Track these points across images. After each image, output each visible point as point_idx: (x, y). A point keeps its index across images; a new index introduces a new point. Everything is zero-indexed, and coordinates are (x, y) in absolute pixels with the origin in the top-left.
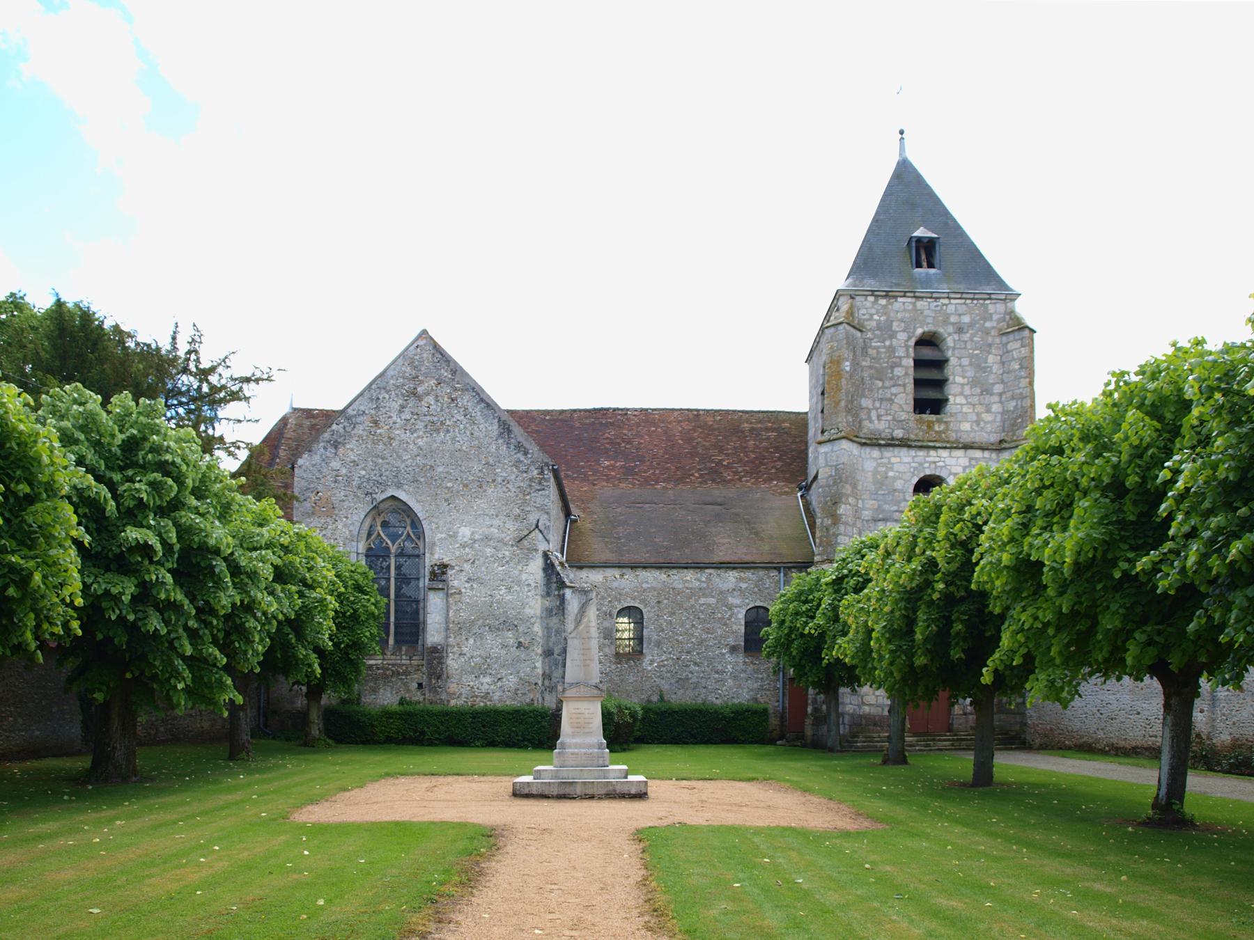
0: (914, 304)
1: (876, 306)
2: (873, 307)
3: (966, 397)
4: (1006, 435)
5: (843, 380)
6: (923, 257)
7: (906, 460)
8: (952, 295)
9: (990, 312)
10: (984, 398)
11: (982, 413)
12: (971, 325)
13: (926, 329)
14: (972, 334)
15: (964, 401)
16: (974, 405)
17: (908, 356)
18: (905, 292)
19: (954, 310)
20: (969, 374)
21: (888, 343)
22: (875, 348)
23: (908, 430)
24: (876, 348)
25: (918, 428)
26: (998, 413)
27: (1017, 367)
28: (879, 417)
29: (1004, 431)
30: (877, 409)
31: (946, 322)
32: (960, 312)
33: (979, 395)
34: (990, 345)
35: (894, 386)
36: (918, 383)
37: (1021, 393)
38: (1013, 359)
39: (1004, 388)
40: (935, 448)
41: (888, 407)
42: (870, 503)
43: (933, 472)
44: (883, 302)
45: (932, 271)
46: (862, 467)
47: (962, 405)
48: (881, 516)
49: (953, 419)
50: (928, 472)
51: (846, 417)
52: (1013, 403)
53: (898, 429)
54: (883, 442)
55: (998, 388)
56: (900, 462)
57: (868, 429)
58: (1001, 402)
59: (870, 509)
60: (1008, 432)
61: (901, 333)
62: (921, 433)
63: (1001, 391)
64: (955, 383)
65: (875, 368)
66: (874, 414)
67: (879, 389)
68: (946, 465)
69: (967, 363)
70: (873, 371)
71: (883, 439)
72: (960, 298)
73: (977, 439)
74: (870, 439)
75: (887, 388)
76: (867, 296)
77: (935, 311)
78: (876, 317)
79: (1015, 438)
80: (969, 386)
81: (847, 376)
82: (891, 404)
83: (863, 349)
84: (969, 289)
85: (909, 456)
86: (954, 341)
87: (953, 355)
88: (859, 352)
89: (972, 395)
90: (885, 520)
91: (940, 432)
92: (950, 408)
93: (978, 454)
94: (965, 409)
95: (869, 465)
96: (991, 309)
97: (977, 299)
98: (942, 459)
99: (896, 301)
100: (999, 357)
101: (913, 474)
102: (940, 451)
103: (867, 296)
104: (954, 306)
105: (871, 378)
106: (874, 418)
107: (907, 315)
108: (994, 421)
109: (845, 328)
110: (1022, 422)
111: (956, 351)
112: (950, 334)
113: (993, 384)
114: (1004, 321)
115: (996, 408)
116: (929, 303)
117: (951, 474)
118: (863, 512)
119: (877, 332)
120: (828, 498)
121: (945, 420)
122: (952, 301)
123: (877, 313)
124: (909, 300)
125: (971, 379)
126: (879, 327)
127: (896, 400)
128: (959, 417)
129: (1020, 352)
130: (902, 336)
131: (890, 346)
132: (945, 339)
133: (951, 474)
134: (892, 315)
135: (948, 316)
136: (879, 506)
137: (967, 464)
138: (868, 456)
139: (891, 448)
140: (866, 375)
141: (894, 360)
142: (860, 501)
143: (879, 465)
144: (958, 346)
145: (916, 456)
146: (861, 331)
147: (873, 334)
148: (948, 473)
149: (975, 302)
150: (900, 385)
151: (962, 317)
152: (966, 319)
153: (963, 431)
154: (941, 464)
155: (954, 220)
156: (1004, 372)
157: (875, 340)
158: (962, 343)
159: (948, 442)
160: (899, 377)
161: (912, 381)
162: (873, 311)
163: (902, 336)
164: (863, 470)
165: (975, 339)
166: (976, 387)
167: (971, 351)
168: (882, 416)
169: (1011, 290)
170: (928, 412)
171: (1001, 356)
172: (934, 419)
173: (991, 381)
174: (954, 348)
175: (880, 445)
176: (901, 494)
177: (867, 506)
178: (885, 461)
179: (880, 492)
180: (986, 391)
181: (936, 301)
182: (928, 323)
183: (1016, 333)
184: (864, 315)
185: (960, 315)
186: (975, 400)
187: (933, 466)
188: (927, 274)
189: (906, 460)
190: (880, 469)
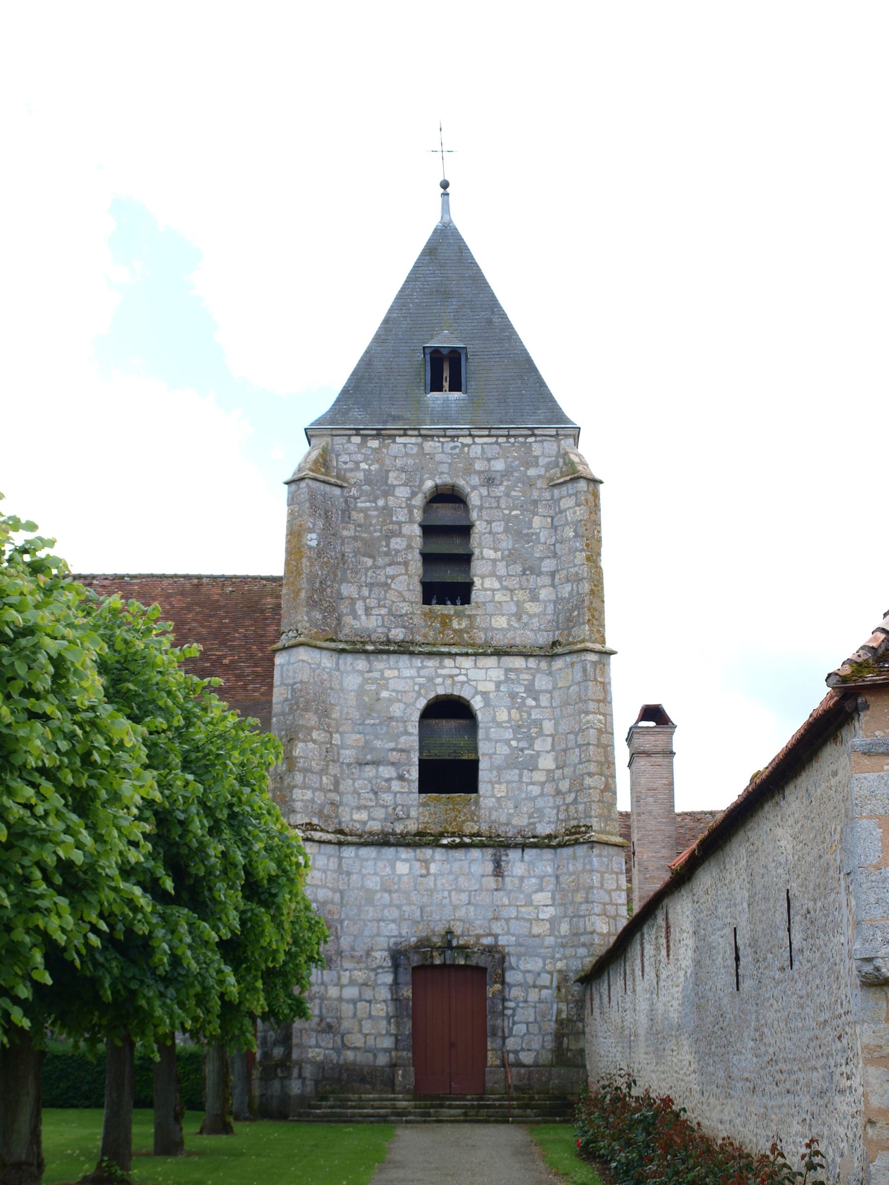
0: (420, 446)
1: (364, 451)
2: (359, 452)
3: (500, 579)
4: (561, 634)
5: (304, 560)
6: (446, 374)
7: (407, 673)
8: (474, 432)
9: (535, 454)
10: (528, 580)
11: (524, 601)
12: (507, 473)
13: (438, 481)
14: (507, 487)
15: (497, 585)
16: (512, 591)
17: (411, 521)
18: (407, 429)
19: (479, 452)
20: (504, 545)
21: (381, 503)
22: (362, 510)
23: (412, 629)
24: (364, 511)
25: (426, 626)
26: (550, 601)
27: (572, 534)
28: (368, 611)
29: (558, 629)
30: (364, 599)
31: (468, 470)
32: (490, 456)
33: (520, 576)
34: (535, 503)
35: (390, 565)
36: (428, 558)
37: (577, 574)
38: (567, 523)
39: (557, 564)
40: (449, 655)
41: (382, 596)
42: (353, 738)
43: (449, 691)
44: (374, 444)
45: (456, 395)
46: (341, 683)
47: (493, 590)
48: (369, 757)
49: (480, 612)
50: (441, 691)
51: (308, 613)
52: (568, 588)
53: (396, 627)
54: (370, 648)
55: (548, 565)
56: (398, 677)
57: (352, 627)
58: (553, 585)
59: (353, 747)
60: (563, 630)
61: (402, 488)
62: (431, 633)
63: (552, 569)
64: (483, 558)
65: (362, 539)
66: (360, 607)
67: (367, 569)
68: (470, 680)
69: (501, 529)
70: (359, 544)
71: (373, 643)
72: (489, 436)
73: (518, 641)
74: (354, 643)
75: (379, 568)
76: (350, 436)
77: (451, 454)
78: (364, 466)
79: (571, 639)
80: (504, 563)
81: (313, 554)
82: (386, 592)
83: (344, 512)
84: (502, 422)
85: (412, 667)
86: (481, 498)
87: (480, 518)
88: (336, 518)
89: (509, 575)
90: (376, 763)
91: (462, 630)
92: (476, 595)
93: (518, 662)
94: (498, 597)
95: (352, 682)
96: (537, 449)
97: (514, 436)
98: (463, 671)
99: (394, 442)
100: (549, 520)
101: (419, 694)
102: (458, 658)
103: (350, 436)
104: (480, 447)
105: (356, 553)
106: (360, 612)
107: (410, 461)
108: (544, 613)
109: (308, 485)
110: (579, 614)
111: (484, 512)
112: (474, 488)
113: (541, 559)
114: (557, 466)
115: (544, 594)
116: (443, 443)
117: (477, 693)
118: (342, 751)
119: (366, 488)
120: (283, 733)
121: (467, 613)
122: (477, 440)
123: (365, 460)
124: (413, 440)
125: (506, 553)
126: (368, 481)
127: (393, 586)
128: (490, 608)
129: (575, 513)
130: (403, 492)
131: (385, 507)
132: (467, 495)
133: (477, 693)
134: (387, 462)
135: (471, 462)
136: (366, 742)
137: (502, 678)
138: (350, 668)
139: (385, 657)
140: (347, 549)
141: (391, 527)
142: (336, 736)
143: (366, 681)
144: (487, 505)
145: (423, 667)
146: (341, 487)
147: (360, 490)
148: (473, 691)
149: (512, 440)
150: (399, 563)
151: (492, 462)
152: (499, 465)
153: (497, 629)
154: (462, 678)
155: (504, 316)
156: (557, 541)
157: (363, 499)
158: (493, 500)
159: (473, 645)
160: (397, 552)
161: (418, 557)
162: (360, 457)
163: (403, 492)
164: (342, 690)
165: (513, 493)
166: (515, 563)
167: (507, 512)
168: (371, 608)
169: (568, 421)
170: (434, 601)
171: (552, 518)
172: (452, 612)
173: (538, 555)
174: (481, 508)
175: (366, 652)
176: (401, 725)
177: (349, 742)
178: (376, 675)
179: (367, 722)
180: (531, 569)
181: (454, 442)
182: (442, 473)
183: (570, 485)
184: (346, 463)
185: (489, 460)
186: (513, 583)
187: (449, 682)
188: (447, 399)
189: (407, 673)
190: (368, 687)
